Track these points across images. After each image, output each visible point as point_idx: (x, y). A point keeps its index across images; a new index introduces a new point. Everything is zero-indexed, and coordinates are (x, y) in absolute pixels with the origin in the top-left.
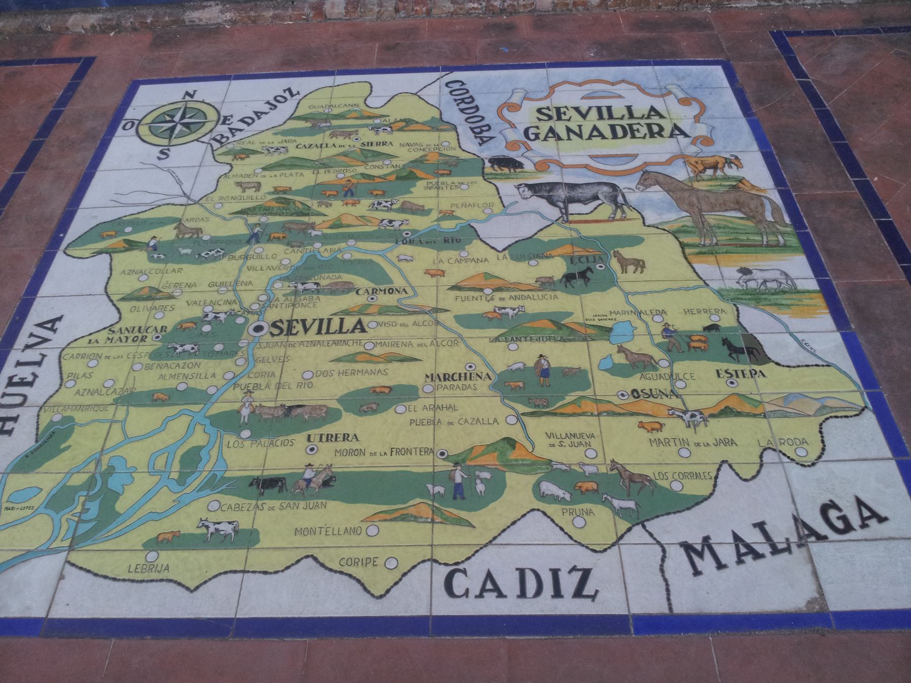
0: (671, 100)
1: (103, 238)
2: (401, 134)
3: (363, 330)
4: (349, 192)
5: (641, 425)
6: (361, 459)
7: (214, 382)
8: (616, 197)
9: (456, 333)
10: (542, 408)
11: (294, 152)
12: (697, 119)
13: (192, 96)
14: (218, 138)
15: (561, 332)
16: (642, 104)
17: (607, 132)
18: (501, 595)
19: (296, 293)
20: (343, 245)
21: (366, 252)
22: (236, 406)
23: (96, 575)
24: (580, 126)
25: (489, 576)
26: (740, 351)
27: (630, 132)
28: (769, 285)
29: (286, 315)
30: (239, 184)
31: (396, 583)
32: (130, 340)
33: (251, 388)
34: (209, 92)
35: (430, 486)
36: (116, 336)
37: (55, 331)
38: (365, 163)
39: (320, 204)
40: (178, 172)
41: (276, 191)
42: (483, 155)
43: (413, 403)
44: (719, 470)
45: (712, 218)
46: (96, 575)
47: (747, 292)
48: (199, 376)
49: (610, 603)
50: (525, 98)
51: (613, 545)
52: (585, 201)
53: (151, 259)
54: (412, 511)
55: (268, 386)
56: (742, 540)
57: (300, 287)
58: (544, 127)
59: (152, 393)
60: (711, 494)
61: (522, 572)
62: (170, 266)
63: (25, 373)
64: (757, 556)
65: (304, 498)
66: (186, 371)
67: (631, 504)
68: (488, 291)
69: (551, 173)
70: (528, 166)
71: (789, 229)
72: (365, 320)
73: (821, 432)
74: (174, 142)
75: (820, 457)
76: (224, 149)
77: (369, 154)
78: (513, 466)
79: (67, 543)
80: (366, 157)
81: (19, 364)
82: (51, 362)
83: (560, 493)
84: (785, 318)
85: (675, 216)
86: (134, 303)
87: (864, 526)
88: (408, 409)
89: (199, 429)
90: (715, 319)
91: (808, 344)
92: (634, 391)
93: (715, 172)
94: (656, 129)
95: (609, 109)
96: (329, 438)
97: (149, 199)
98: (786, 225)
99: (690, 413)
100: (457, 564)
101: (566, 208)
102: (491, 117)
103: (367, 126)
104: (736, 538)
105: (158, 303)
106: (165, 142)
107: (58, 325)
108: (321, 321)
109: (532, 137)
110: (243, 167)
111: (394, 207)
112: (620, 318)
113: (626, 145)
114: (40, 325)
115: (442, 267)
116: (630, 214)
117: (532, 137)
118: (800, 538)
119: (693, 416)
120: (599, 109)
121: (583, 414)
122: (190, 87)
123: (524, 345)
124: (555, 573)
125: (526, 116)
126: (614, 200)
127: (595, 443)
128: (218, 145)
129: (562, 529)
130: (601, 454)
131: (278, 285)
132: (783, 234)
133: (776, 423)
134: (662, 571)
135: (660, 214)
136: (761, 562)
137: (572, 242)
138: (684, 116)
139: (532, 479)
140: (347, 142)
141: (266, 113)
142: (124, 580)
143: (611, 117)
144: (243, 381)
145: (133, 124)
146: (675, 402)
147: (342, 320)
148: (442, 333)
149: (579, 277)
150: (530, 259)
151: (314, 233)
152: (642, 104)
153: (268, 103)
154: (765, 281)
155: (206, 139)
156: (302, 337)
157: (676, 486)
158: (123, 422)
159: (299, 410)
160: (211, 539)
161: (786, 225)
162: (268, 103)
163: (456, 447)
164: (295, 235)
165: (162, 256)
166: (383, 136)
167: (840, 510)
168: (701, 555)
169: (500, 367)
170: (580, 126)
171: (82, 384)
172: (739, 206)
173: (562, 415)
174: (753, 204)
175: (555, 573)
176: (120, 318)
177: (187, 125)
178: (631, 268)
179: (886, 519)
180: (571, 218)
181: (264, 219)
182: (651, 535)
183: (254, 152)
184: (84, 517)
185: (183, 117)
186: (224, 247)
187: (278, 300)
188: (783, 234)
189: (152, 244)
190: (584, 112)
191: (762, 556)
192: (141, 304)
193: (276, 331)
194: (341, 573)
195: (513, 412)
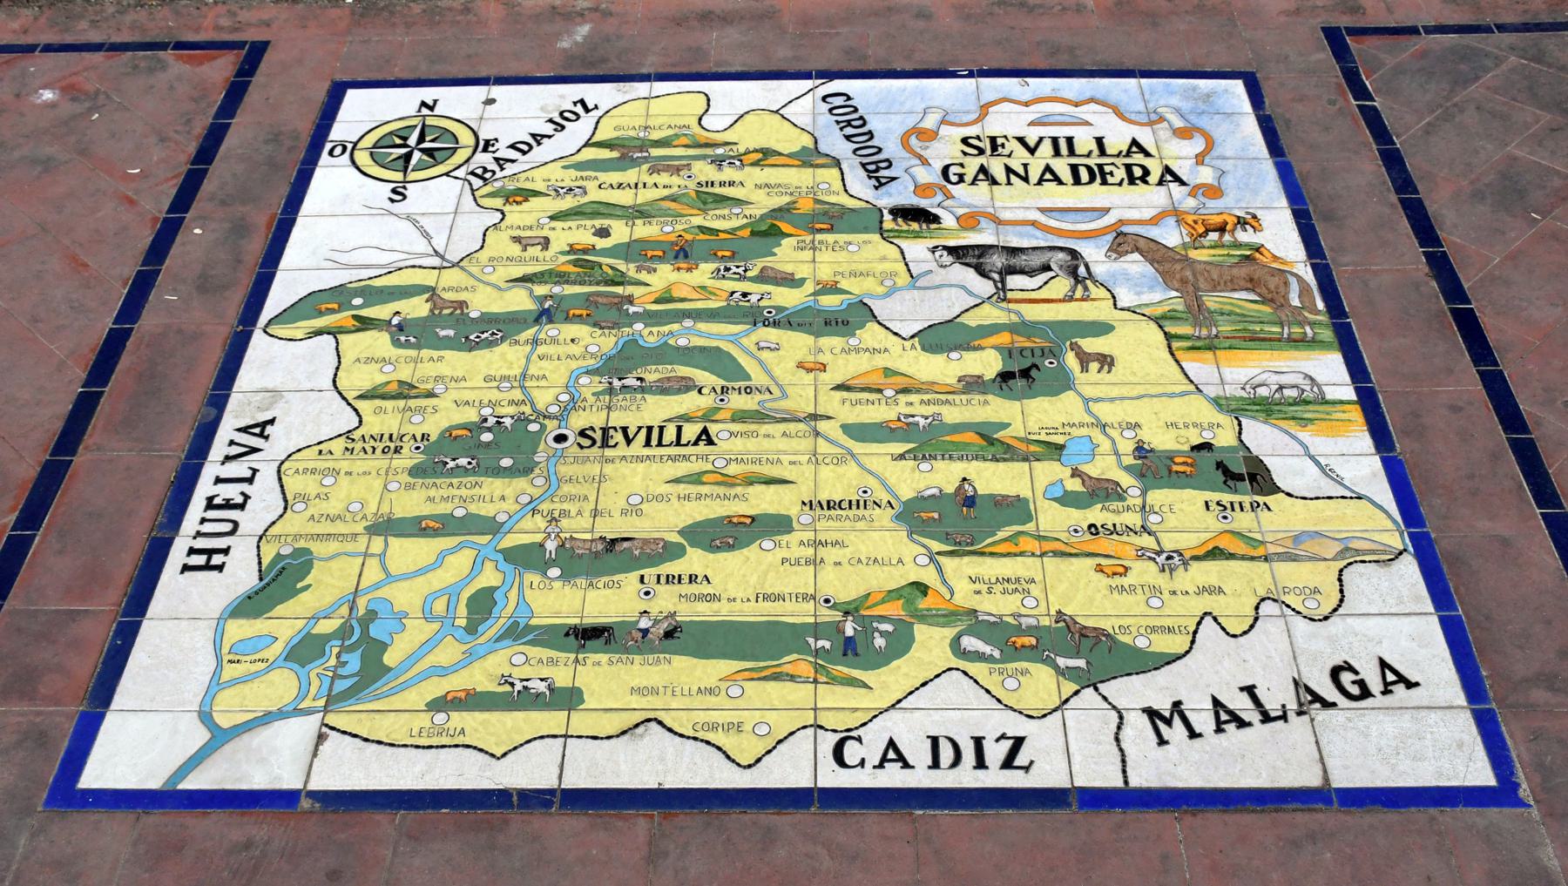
0: (1163, 131)
1: (321, 313)
2: (757, 170)
3: (710, 442)
4: (682, 253)
5: (1100, 569)
6: (715, 605)
7: (505, 506)
8: (1076, 267)
9: (842, 447)
10: (964, 546)
11: (595, 195)
12: (1200, 159)
13: (431, 108)
14: (479, 171)
15: (992, 449)
16: (1118, 139)
17: (1066, 175)
18: (906, 765)
19: (611, 391)
20: (675, 327)
21: (709, 336)
22: (538, 538)
23: (366, 740)
24: (1025, 166)
25: (891, 744)
26: (1240, 478)
27: (1099, 175)
28: (1287, 392)
29: (596, 419)
30: (517, 239)
31: (769, 752)
32: (378, 451)
33: (556, 514)
34: (457, 103)
35: (811, 640)
36: (358, 446)
37: (267, 438)
38: (705, 211)
39: (639, 270)
40: (424, 222)
41: (572, 250)
42: (881, 203)
43: (785, 538)
44: (1199, 623)
45: (1212, 301)
46: (366, 740)
47: (1256, 401)
48: (481, 498)
49: (1047, 773)
50: (943, 122)
51: (1055, 710)
52: (1030, 273)
53: (396, 343)
54: (787, 669)
55: (580, 513)
57: (617, 383)
58: (972, 165)
59: (419, 520)
60: (1187, 652)
61: (935, 741)
62: (426, 353)
63: (232, 492)
64: (1242, 724)
65: (640, 651)
66: (464, 492)
67: (1081, 663)
68: (889, 393)
69: (981, 231)
70: (948, 220)
71: (1323, 318)
72: (713, 429)
73: (1340, 580)
74: (412, 176)
75: (1335, 610)
76: (488, 189)
77: (708, 199)
78: (925, 617)
79: (322, 702)
80: (705, 203)
81: (218, 480)
82: (267, 477)
83: (987, 649)
84: (1304, 435)
85: (1162, 297)
86: (378, 402)
87: (1386, 692)
88: (778, 545)
89: (489, 566)
90: (1207, 436)
91: (1333, 471)
92: (1091, 526)
93: (1221, 236)
94: (1138, 172)
95: (1070, 140)
96: (669, 579)
97: (385, 258)
98: (1318, 312)
99: (1164, 556)
100: (848, 730)
101: (1003, 281)
102: (892, 148)
103: (704, 157)
104: (1216, 703)
105: (412, 403)
106: (399, 176)
107: (269, 430)
108: (650, 429)
109: (954, 179)
110: (521, 216)
111: (749, 274)
112: (1075, 432)
113: (1092, 195)
114: (244, 430)
115: (822, 358)
116: (1095, 291)
117: (954, 179)
118: (1300, 704)
119: (1169, 558)
120: (1055, 141)
121: (1021, 554)
122: (428, 94)
123: (940, 465)
124: (978, 742)
125: (947, 149)
126: (1073, 272)
127: (1035, 590)
128: (480, 183)
129: (988, 691)
130: (1043, 604)
131: (584, 380)
132: (1312, 324)
133: (1283, 569)
134: (1117, 739)
135: (1138, 294)
136: (1247, 730)
137: (1012, 328)
138: (1180, 154)
139: (950, 633)
140: (675, 180)
141: (550, 137)
142: (405, 746)
143: (1072, 152)
144: (545, 507)
145: (345, 148)
146: (1147, 541)
147: (679, 429)
148: (823, 447)
149: (1020, 376)
150: (951, 350)
151: (632, 309)
152: (1118, 139)
153: (551, 121)
154: (1281, 388)
155: (461, 173)
156: (622, 450)
157: (1141, 643)
158: (382, 556)
159: (626, 544)
160: (518, 698)
161: (1318, 312)
162: (551, 121)
163: (846, 592)
164: (606, 311)
165: (412, 340)
166: (728, 173)
167: (1357, 673)
168: (1169, 722)
169: (907, 493)
170: (1025, 166)
171: (317, 508)
172: (1252, 284)
173: (992, 554)
174: (1273, 282)
175: (978, 742)
176: (361, 422)
177: (429, 152)
178: (1094, 366)
179: (1417, 684)
180: (1010, 295)
181: (557, 290)
182: (1105, 698)
183: (536, 194)
184: (340, 671)
185: (421, 139)
186: (501, 327)
187: (585, 400)
188: (1312, 324)
189: (395, 321)
190: (1032, 144)
191: (1249, 724)
192: (389, 404)
193: (586, 442)
194: (695, 739)
195: (924, 551)
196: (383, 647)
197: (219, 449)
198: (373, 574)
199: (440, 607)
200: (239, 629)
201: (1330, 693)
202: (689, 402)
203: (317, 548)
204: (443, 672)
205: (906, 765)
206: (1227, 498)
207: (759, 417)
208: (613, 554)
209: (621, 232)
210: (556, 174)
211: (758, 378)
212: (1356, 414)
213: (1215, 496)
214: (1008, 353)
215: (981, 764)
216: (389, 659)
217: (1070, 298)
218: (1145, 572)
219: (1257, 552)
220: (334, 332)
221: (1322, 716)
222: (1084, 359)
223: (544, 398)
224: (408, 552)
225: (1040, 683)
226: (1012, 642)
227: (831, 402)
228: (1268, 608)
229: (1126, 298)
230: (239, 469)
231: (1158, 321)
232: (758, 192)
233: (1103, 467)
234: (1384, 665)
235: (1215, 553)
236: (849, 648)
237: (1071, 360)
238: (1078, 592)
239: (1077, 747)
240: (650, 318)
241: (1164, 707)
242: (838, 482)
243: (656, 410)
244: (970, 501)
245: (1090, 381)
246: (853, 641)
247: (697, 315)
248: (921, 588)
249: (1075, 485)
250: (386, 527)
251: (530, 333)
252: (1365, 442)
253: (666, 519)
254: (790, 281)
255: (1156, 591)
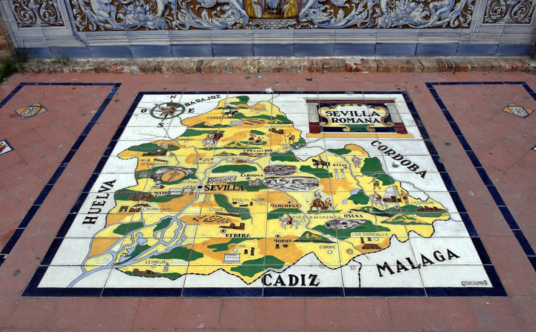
56: (400, 264)
64: (406, 269)
104: (398, 263)
179: (459, 257)
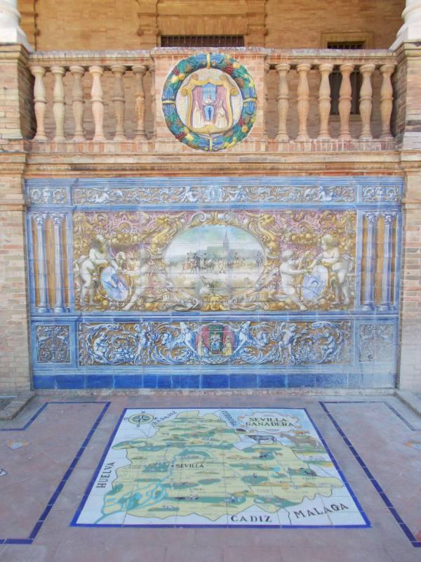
0: (288, 417)
11: (177, 427)
16: (280, 418)
58: (252, 422)
77: (199, 427)
113: (276, 427)
125: (246, 419)
138: (293, 421)
152: (280, 418)
196: (139, 500)
197: (103, 467)
198: (135, 488)
199: (150, 494)
200: (108, 497)
201: (331, 509)
202: (198, 460)
203: (124, 484)
204: (151, 504)
205: (246, 521)
206: (308, 477)
207: (212, 463)
208: (184, 485)
209: (183, 432)
210: (169, 423)
211: (212, 456)
212: (332, 464)
213: (305, 477)
214: (261, 453)
215: (261, 520)
216: (140, 502)
217: (273, 444)
218: (291, 489)
219: (313, 486)
220: (126, 448)
221: (329, 513)
222: (277, 454)
223: (169, 459)
224: (141, 484)
225: (272, 507)
226: (265, 500)
227: (227, 461)
228: (317, 495)
229: (284, 444)
230: (108, 471)
231: (291, 448)
232: (210, 426)
233: (281, 472)
234: (341, 505)
235: (306, 486)
236: (233, 501)
237: (274, 454)
238: (279, 492)
239: (280, 517)
240: (189, 446)
241: (298, 511)
242: (228, 474)
243: (192, 461)
244: (256, 477)
245: (278, 457)
246: (233, 500)
247: (199, 446)
248: (247, 491)
249: (277, 475)
250: (138, 480)
251: (166, 448)
252: (334, 467)
253: (195, 480)
254: (217, 440)
255: (294, 492)
